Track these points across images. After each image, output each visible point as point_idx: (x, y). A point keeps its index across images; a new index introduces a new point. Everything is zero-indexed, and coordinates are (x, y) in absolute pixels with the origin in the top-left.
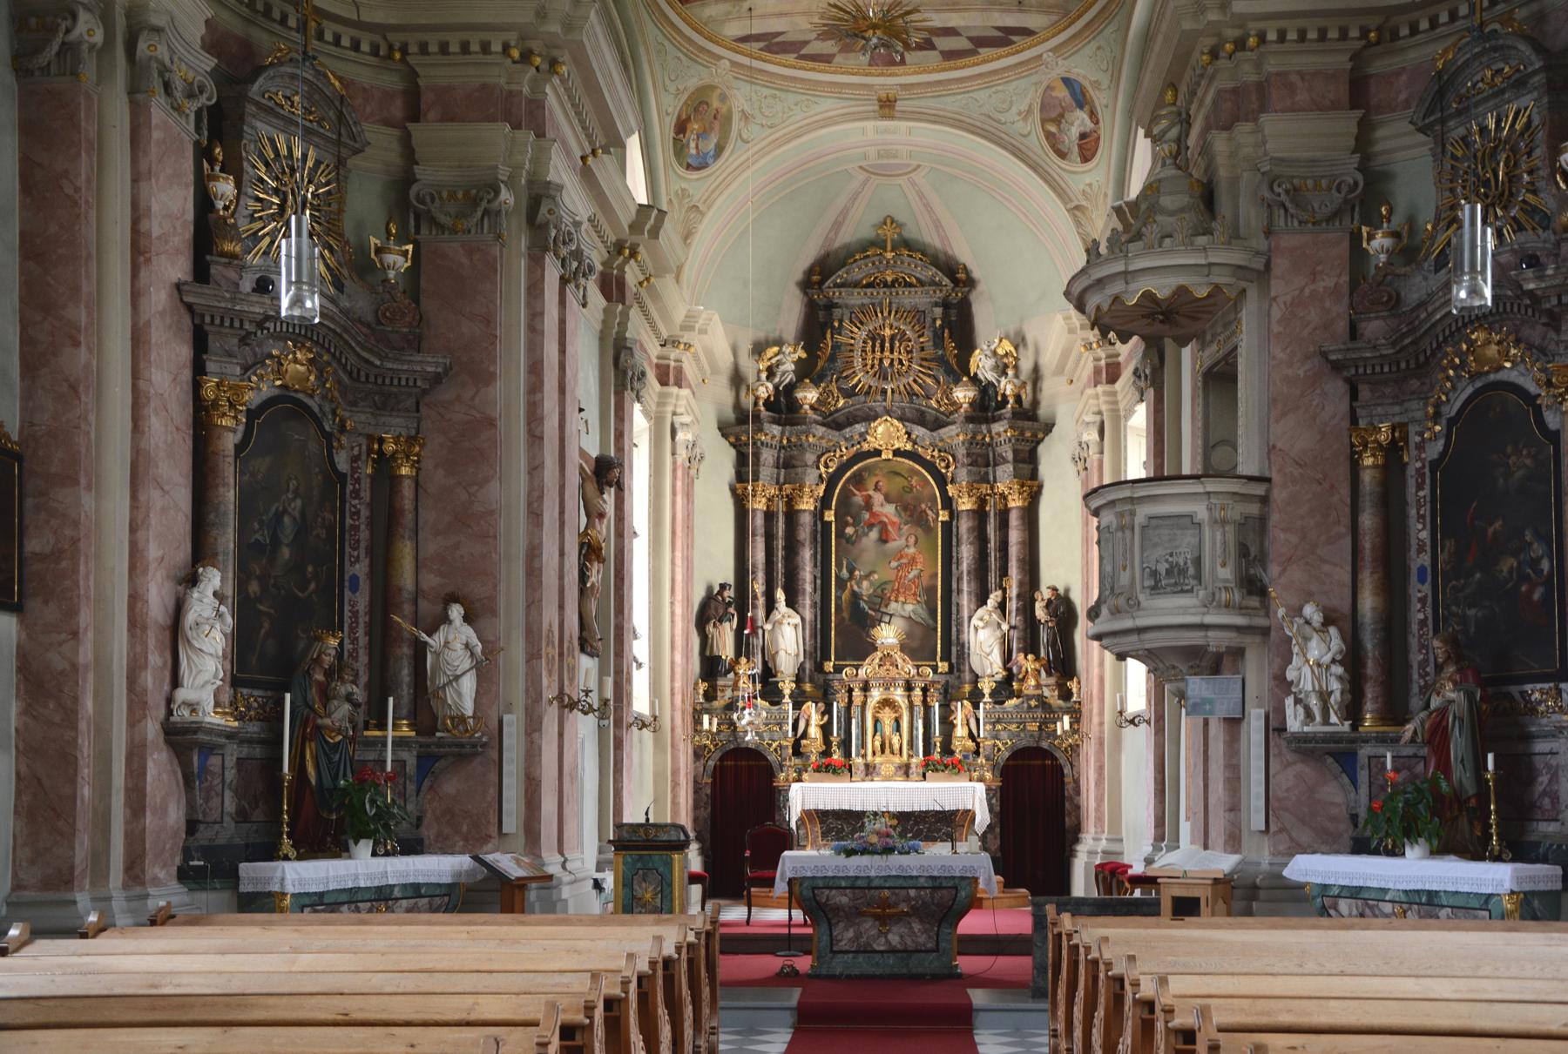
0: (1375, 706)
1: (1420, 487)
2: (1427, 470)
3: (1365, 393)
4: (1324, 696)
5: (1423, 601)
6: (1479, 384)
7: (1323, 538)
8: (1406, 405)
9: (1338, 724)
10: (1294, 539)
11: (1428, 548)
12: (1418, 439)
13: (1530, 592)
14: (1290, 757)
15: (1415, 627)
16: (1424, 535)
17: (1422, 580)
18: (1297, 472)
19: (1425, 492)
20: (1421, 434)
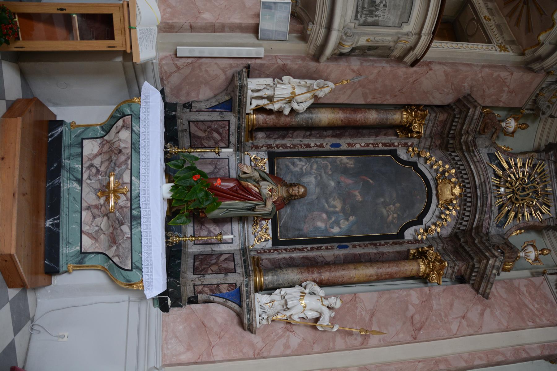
0: (261, 122)
1: (384, 145)
2: (392, 148)
3: (442, 117)
4: (270, 99)
5: (321, 146)
6: (432, 183)
7: (368, 91)
8: (429, 140)
9: (252, 105)
10: (371, 77)
11: (350, 148)
12: (410, 144)
13: (322, 220)
14: (230, 73)
15: (306, 141)
16: (358, 146)
17: (332, 146)
18: (411, 80)
19: (381, 147)
20: (412, 145)
